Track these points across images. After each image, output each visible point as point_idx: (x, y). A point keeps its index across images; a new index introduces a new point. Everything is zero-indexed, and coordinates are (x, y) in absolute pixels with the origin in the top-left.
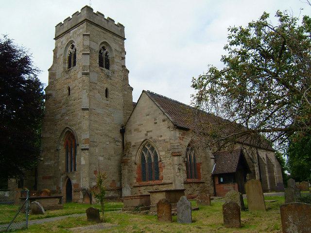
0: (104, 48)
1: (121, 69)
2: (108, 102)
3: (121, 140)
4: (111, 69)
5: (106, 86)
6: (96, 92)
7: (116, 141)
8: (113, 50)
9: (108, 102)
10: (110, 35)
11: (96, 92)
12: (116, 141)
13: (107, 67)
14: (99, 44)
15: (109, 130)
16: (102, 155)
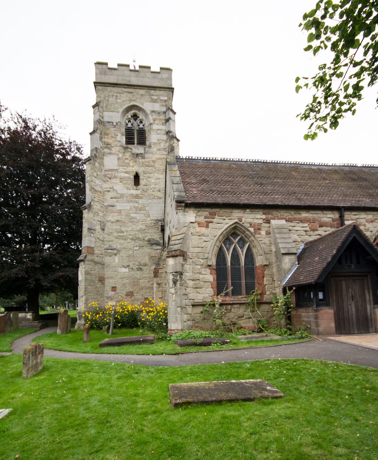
0: (135, 117)
1: (165, 137)
2: (138, 192)
3: (162, 241)
4: (147, 143)
5: (135, 168)
6: (118, 181)
7: (152, 243)
8: (148, 112)
9: (138, 192)
10: (142, 92)
11: (118, 181)
12: (152, 243)
13: (142, 141)
14: (121, 110)
15: (140, 231)
16: (125, 265)
